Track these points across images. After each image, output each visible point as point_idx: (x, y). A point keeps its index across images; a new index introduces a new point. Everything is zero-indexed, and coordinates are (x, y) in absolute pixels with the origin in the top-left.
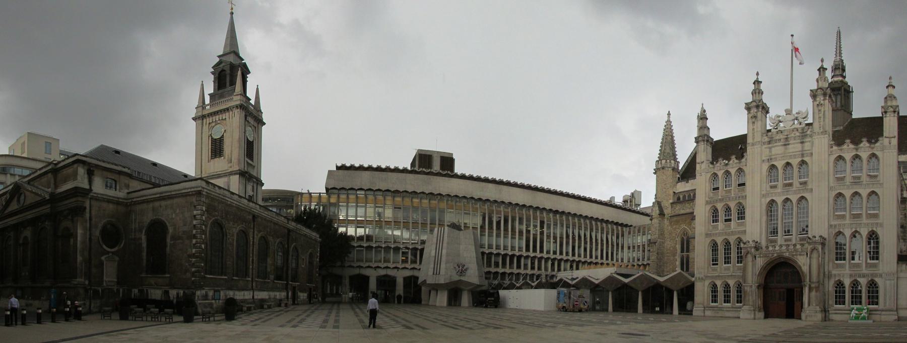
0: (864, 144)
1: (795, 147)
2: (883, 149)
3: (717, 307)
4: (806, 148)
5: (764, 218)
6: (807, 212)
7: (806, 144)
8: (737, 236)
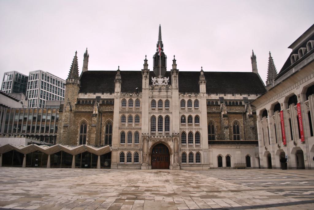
0: (193, 95)
1: (164, 93)
2: (201, 97)
3: (124, 164)
4: (168, 94)
5: (150, 123)
6: (169, 122)
7: (169, 93)
8: (136, 130)
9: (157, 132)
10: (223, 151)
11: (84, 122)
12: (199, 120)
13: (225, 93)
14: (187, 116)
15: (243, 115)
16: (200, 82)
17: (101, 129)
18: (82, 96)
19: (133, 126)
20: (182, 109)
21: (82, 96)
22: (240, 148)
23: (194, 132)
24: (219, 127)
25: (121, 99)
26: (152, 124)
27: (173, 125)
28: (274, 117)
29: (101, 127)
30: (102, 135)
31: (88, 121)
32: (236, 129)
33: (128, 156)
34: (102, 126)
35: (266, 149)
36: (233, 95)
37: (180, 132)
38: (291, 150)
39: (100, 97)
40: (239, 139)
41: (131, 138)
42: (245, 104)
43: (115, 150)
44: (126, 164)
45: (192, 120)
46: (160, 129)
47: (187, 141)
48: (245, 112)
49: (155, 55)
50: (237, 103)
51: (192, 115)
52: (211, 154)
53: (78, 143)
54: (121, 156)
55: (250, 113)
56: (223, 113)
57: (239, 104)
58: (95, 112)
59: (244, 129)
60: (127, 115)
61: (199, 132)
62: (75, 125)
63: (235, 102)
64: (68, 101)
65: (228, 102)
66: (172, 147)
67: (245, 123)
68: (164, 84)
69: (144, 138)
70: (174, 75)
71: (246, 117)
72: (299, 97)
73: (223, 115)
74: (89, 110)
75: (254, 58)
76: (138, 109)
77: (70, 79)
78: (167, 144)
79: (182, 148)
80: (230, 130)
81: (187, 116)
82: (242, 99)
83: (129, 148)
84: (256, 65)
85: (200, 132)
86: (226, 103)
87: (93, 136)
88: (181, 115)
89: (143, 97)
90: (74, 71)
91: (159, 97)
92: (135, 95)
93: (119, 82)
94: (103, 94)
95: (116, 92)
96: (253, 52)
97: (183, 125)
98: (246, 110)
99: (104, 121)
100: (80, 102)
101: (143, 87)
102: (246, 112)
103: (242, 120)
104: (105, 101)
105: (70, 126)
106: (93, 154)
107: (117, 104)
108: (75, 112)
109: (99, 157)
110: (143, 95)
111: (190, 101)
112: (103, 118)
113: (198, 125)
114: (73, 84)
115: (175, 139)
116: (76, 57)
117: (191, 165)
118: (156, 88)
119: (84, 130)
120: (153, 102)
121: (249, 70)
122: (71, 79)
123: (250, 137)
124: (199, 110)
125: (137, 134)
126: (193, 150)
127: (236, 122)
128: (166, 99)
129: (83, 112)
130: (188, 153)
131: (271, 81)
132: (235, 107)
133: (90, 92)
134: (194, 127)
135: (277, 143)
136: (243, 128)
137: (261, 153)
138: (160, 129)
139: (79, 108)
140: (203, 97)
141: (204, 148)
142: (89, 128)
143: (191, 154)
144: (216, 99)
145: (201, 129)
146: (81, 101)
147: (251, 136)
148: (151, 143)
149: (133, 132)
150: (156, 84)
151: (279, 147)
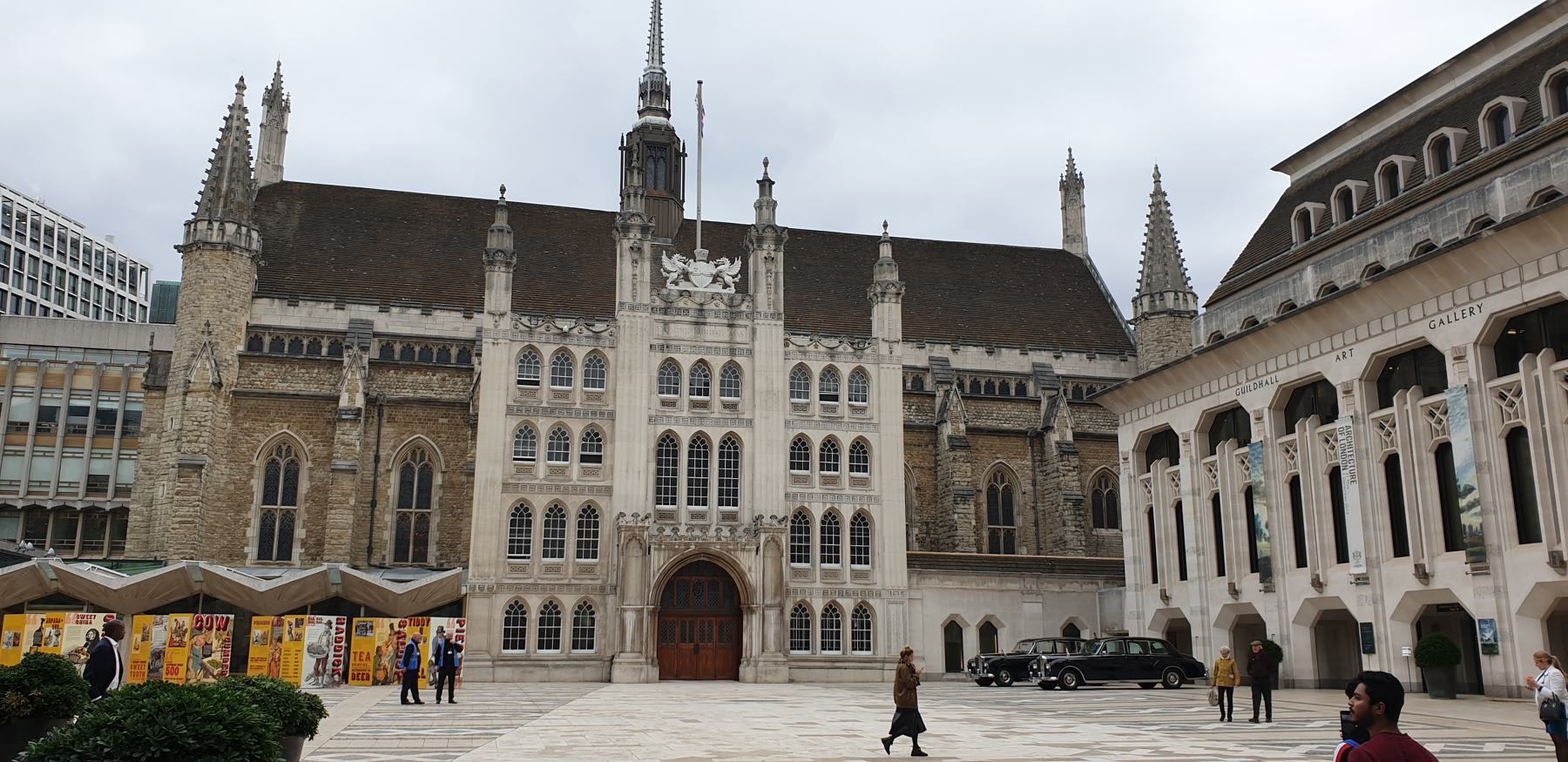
1: (716, 332)
5: (653, 466)
7: (739, 331)
8: (586, 498)
9: (683, 508)
10: (968, 600)
11: (283, 447)
12: (865, 460)
13: (958, 340)
14: (817, 438)
15: (1032, 445)
16: (879, 289)
17: (375, 482)
18: (274, 314)
19: (575, 476)
20: (795, 407)
21: (274, 314)
22: (1038, 593)
23: (847, 513)
24: (929, 493)
25: (517, 347)
26: (659, 471)
27: (757, 476)
28: (1213, 464)
29: (375, 475)
30: (383, 512)
31: (305, 440)
32: (1000, 504)
33: (542, 621)
34: (381, 469)
35: (1165, 597)
36: (990, 353)
37: (787, 508)
38: (1294, 607)
39: (370, 324)
40: (1010, 548)
41: (562, 534)
42: (1040, 394)
43: (481, 589)
44: (533, 656)
45: (836, 458)
46: (698, 495)
47: (816, 552)
48: (1039, 427)
49: (629, 134)
50: (1005, 387)
51: (838, 434)
52: (915, 613)
53: (252, 550)
54: (507, 621)
55: (1063, 436)
56: (947, 430)
57: (1013, 392)
58: (351, 400)
59: (1035, 502)
60: (544, 426)
61: (868, 513)
62: (235, 458)
63: (997, 384)
64: (205, 338)
65: (967, 383)
66: (754, 577)
67: (1039, 478)
68: (717, 288)
69: (633, 537)
70: (765, 254)
71: (1043, 452)
72: (1348, 392)
73: (950, 438)
74: (313, 389)
75: (1072, 186)
76: (598, 396)
77: (210, 223)
78: (734, 565)
79: (792, 585)
80: (977, 505)
81: (817, 438)
82: (1027, 369)
83: (552, 578)
84: (1082, 220)
85: (874, 511)
86: (961, 386)
87: (341, 519)
88: (793, 434)
89: (623, 345)
90: (231, 180)
91: (694, 349)
92: (586, 332)
93: (508, 265)
95: (490, 313)
96: (1071, 160)
97: (797, 480)
98: (1047, 418)
99: (393, 442)
100: (262, 344)
101: (623, 293)
102: (1048, 428)
103: (1029, 463)
104: (398, 347)
105: (212, 467)
107: (497, 371)
108: (234, 393)
110: (624, 335)
111: (830, 373)
112: (387, 430)
113: (864, 483)
114: (229, 247)
115: (767, 542)
116: (238, 109)
117: (833, 663)
118: (681, 305)
119: (285, 489)
120: (669, 372)
121: (1055, 242)
122: (216, 225)
123: (1061, 543)
124: (868, 413)
125: (589, 516)
126: (841, 595)
127: (1000, 473)
128: (727, 359)
130: (818, 606)
131: (1157, 297)
132: (1001, 405)
133: (318, 297)
134: (848, 491)
135: (1221, 572)
136: (1029, 498)
137: (1140, 616)
138: (698, 495)
139: (261, 374)
140: (890, 353)
141: (888, 585)
142: (311, 478)
143: (832, 610)
144: (919, 364)
145: (877, 500)
146: (267, 340)
147: (1069, 536)
148: (659, 561)
149: (573, 505)
150: (683, 286)
151: (1234, 591)
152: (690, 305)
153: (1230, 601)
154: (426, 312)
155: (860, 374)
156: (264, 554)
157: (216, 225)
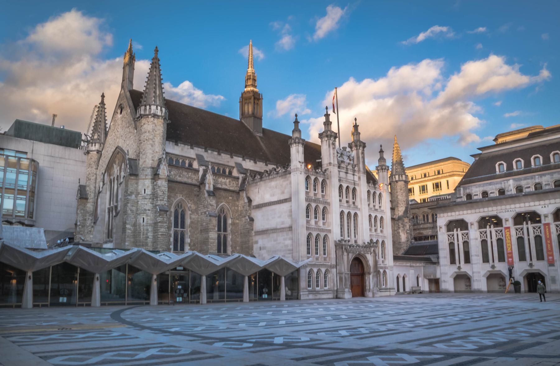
7: (355, 177)
8: (325, 234)
39: (202, 156)
51: (378, 215)
58: (209, 187)
78: (365, 258)
94: (206, 151)
106: (275, 274)
109: (204, 279)
129: (185, 183)
133: (185, 143)
142: (191, 218)
149: (322, 234)
152: (345, 166)
153: (490, 269)
154: (219, 154)
155: (380, 194)
156: (175, 249)
157: (159, 108)
